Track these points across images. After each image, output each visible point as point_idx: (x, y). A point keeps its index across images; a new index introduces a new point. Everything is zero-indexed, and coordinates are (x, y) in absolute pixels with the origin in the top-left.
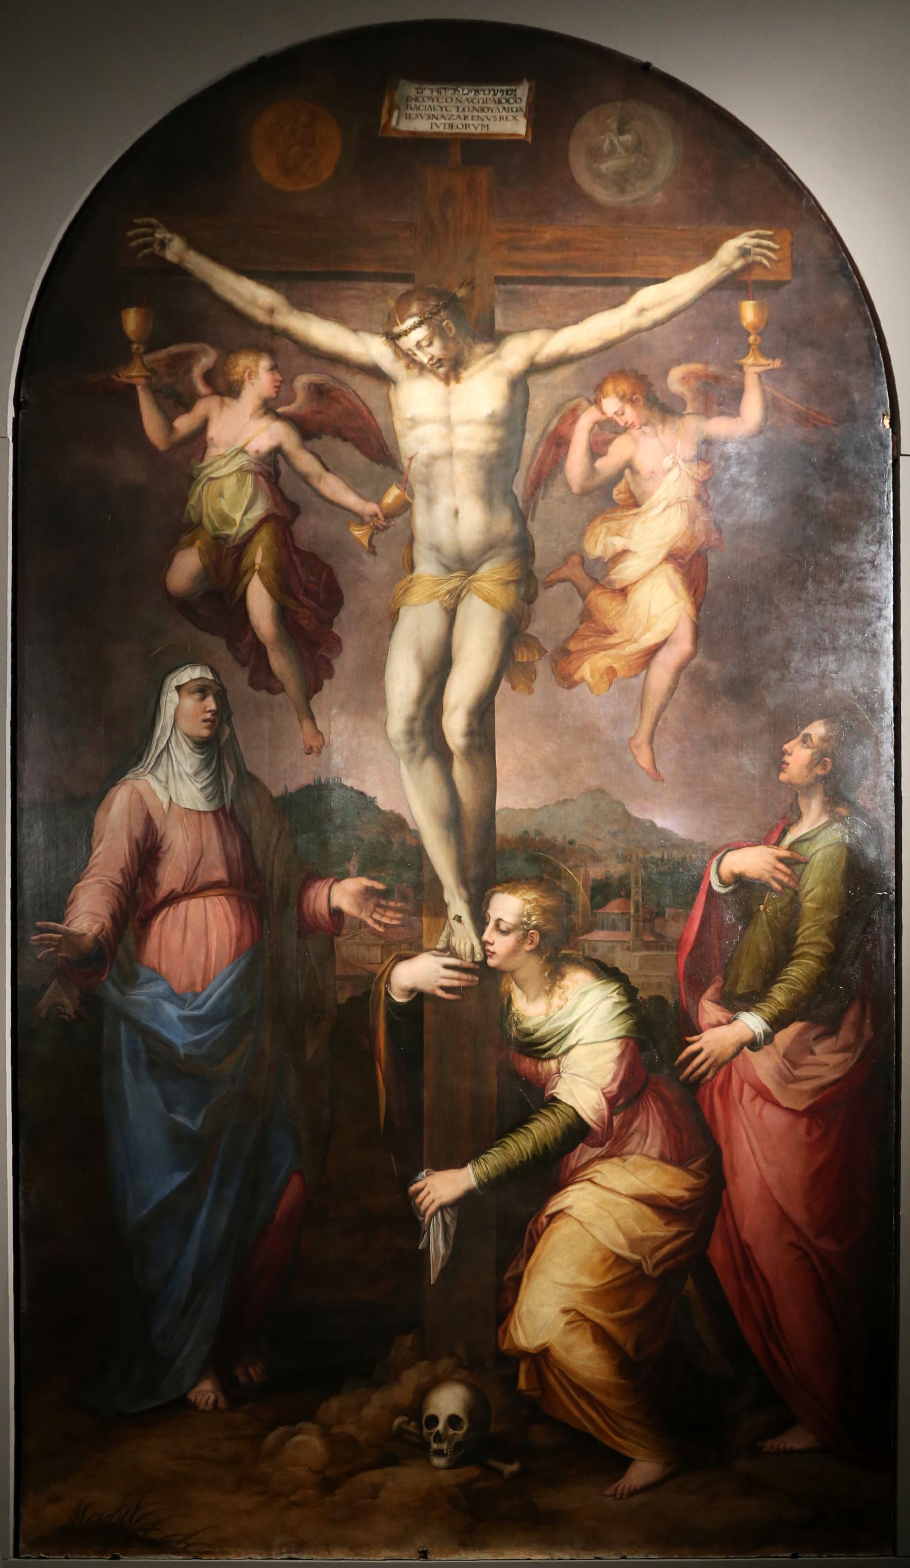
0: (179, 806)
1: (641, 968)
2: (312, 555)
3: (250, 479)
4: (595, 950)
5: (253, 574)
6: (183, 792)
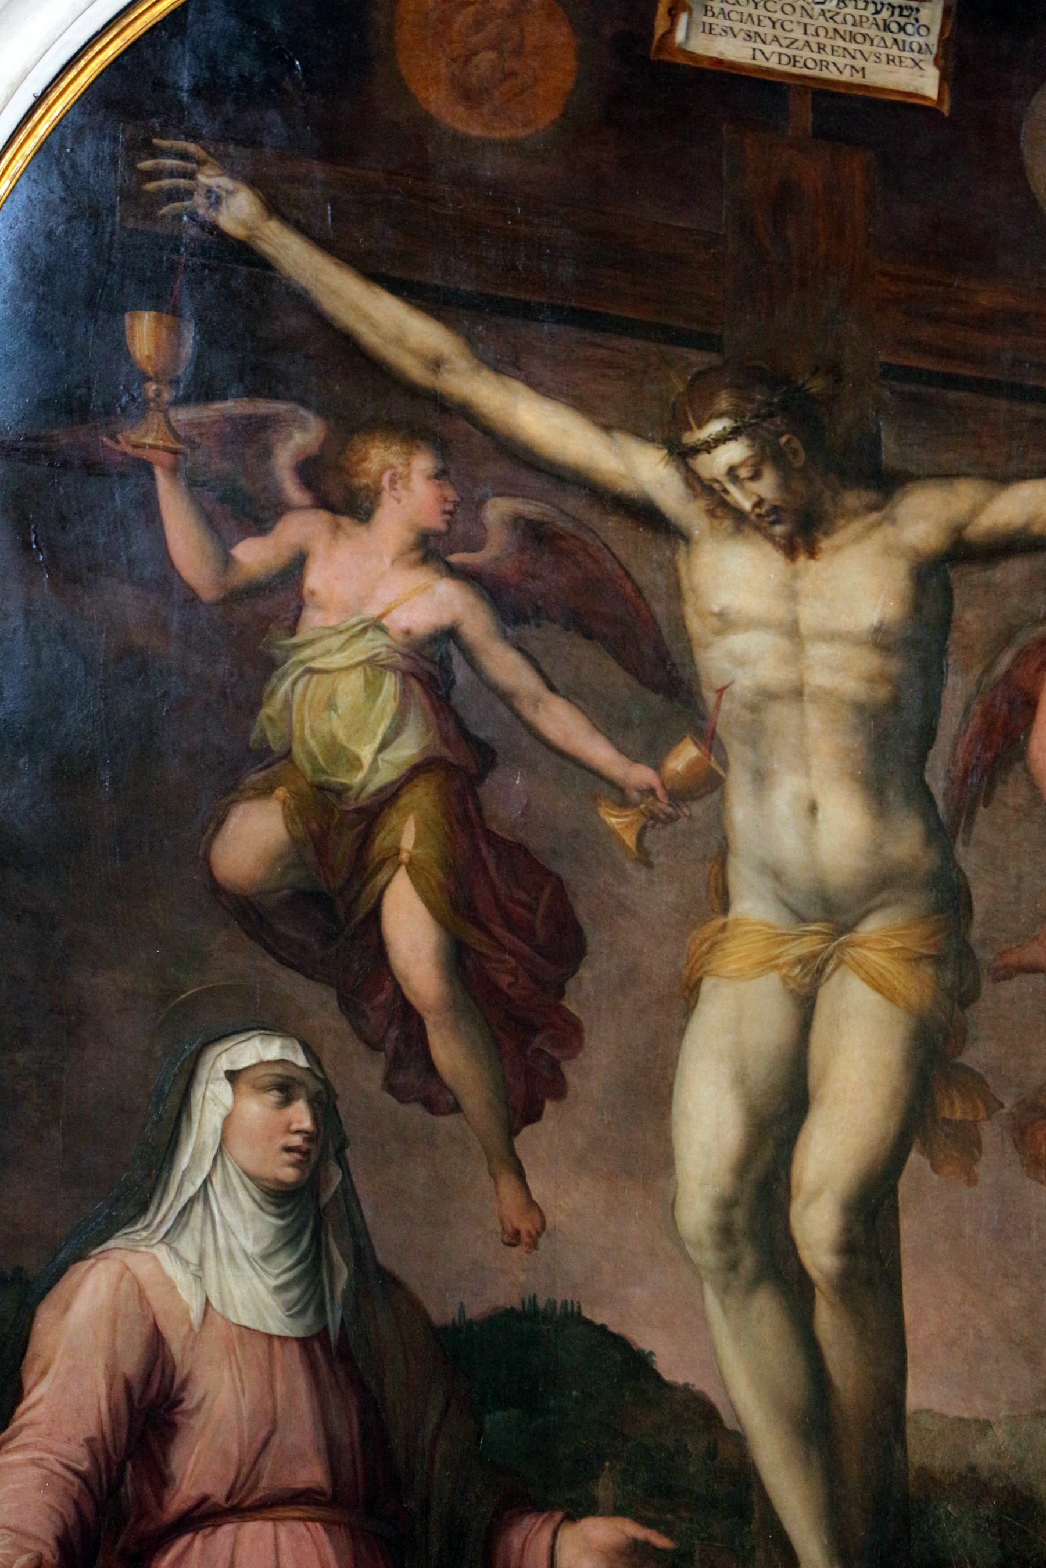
0: (225, 1318)
2: (522, 848)
3: (390, 684)
5: (396, 871)
6: (237, 1292)
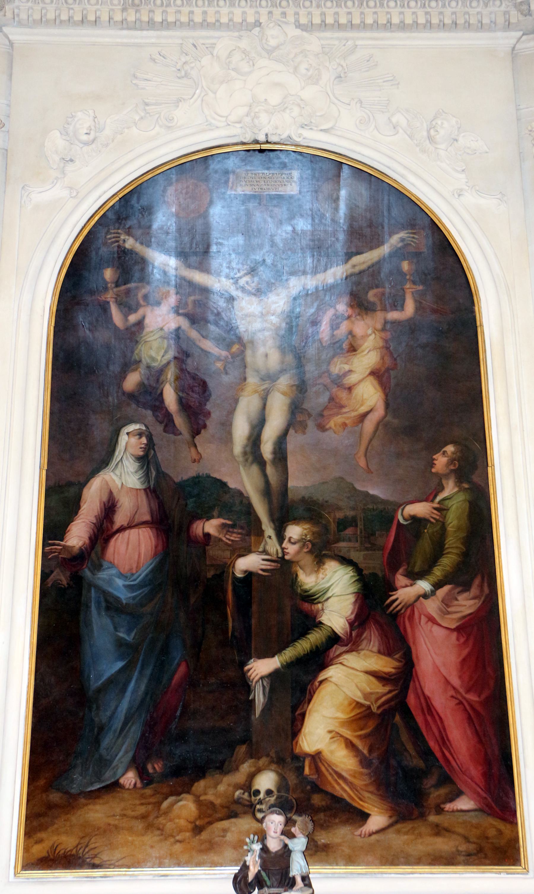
1: (365, 559)
4: (340, 551)
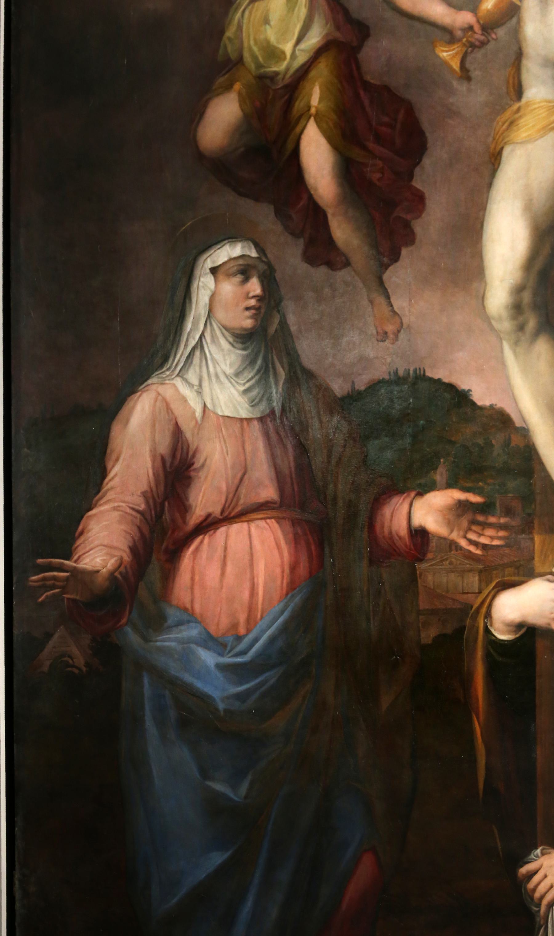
0: (217, 414)
2: (386, 88)
